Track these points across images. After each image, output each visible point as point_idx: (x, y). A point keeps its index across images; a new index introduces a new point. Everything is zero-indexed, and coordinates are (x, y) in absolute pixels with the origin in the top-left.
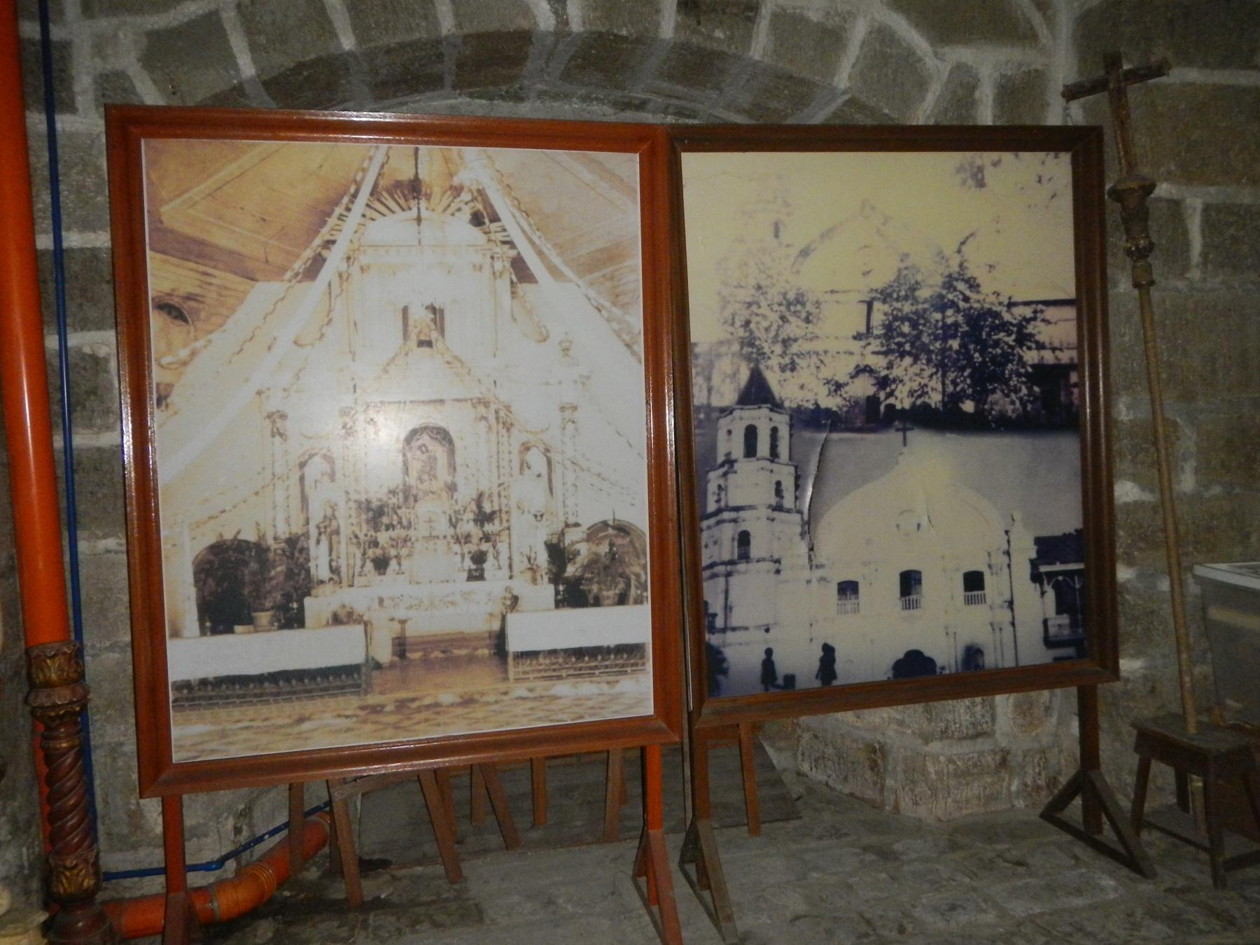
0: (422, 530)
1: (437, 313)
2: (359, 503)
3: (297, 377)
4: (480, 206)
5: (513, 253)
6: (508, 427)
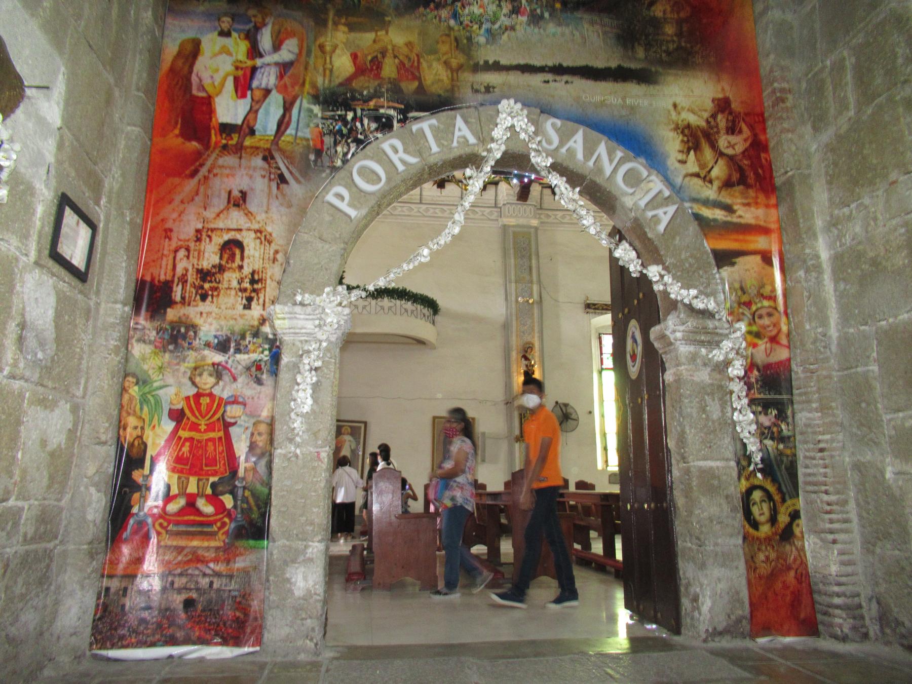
0: (225, 285)
1: (244, 194)
2: (197, 270)
3: (180, 216)
4: (267, 154)
5: (279, 172)
6: (270, 242)
